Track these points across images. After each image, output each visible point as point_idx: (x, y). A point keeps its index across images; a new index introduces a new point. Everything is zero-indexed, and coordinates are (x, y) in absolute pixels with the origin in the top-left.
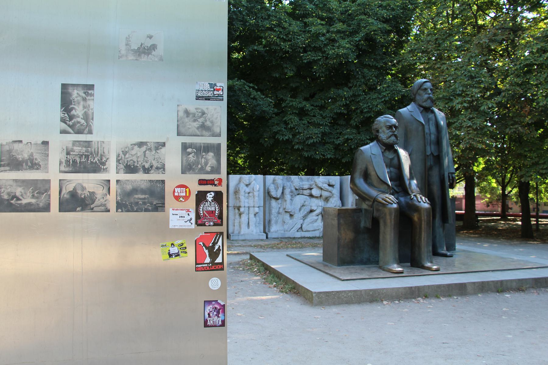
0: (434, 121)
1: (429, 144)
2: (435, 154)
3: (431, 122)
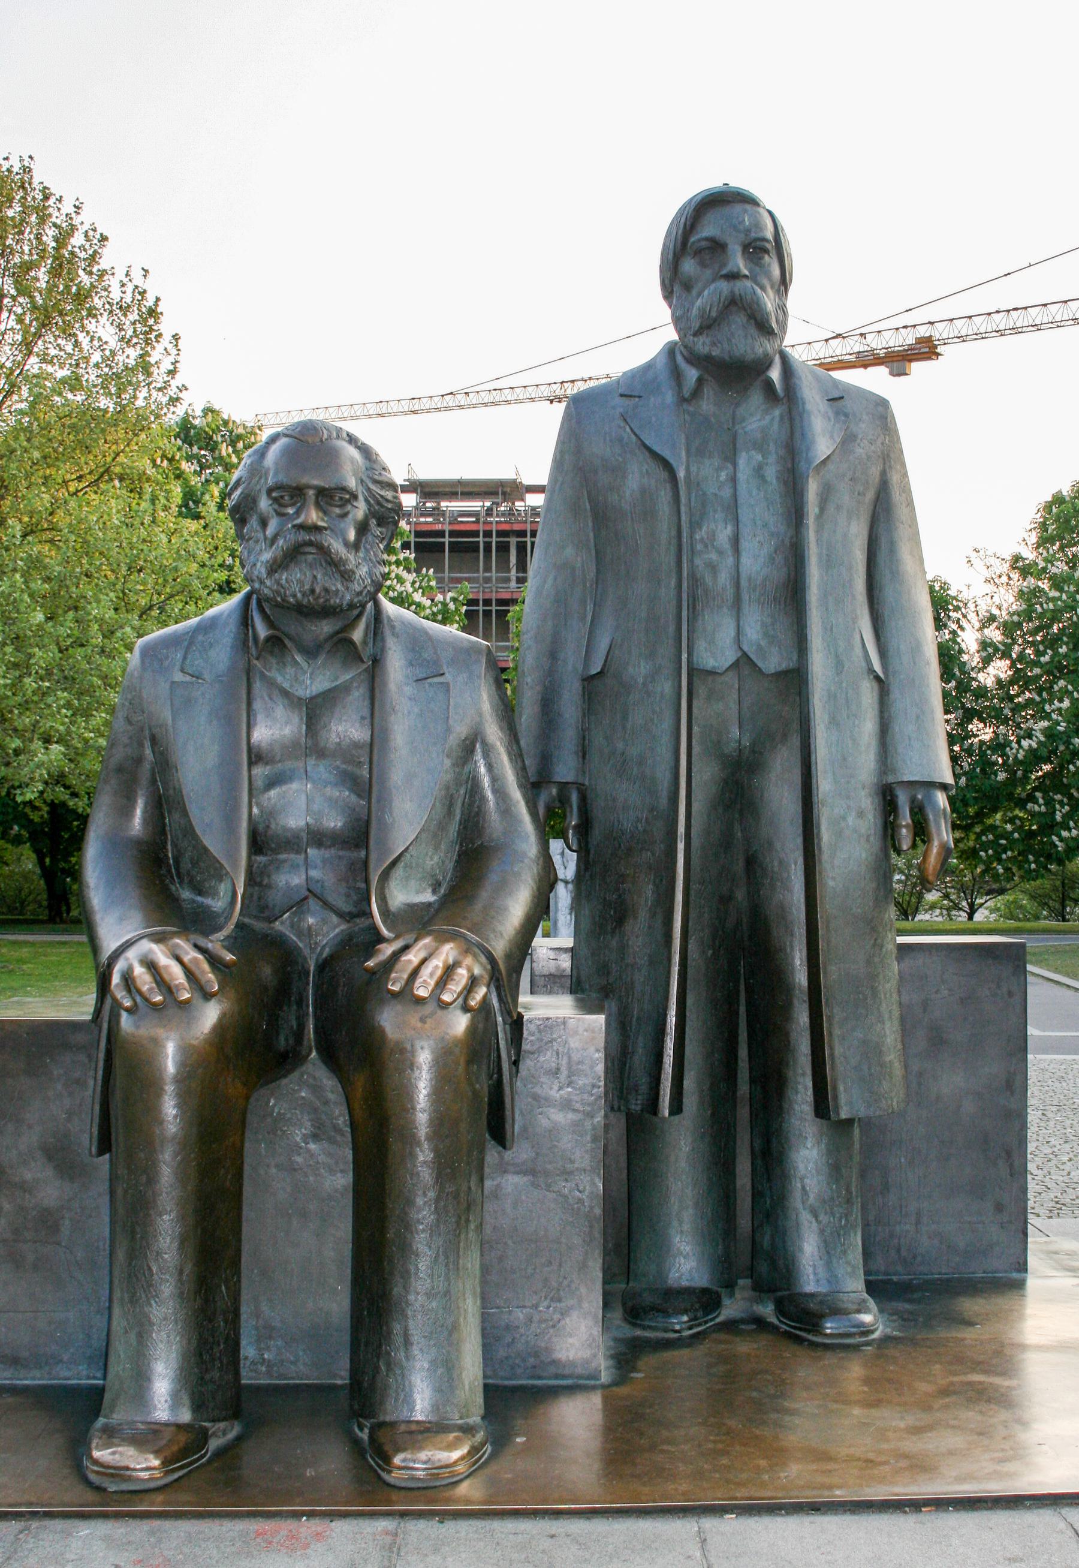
2: (773, 662)
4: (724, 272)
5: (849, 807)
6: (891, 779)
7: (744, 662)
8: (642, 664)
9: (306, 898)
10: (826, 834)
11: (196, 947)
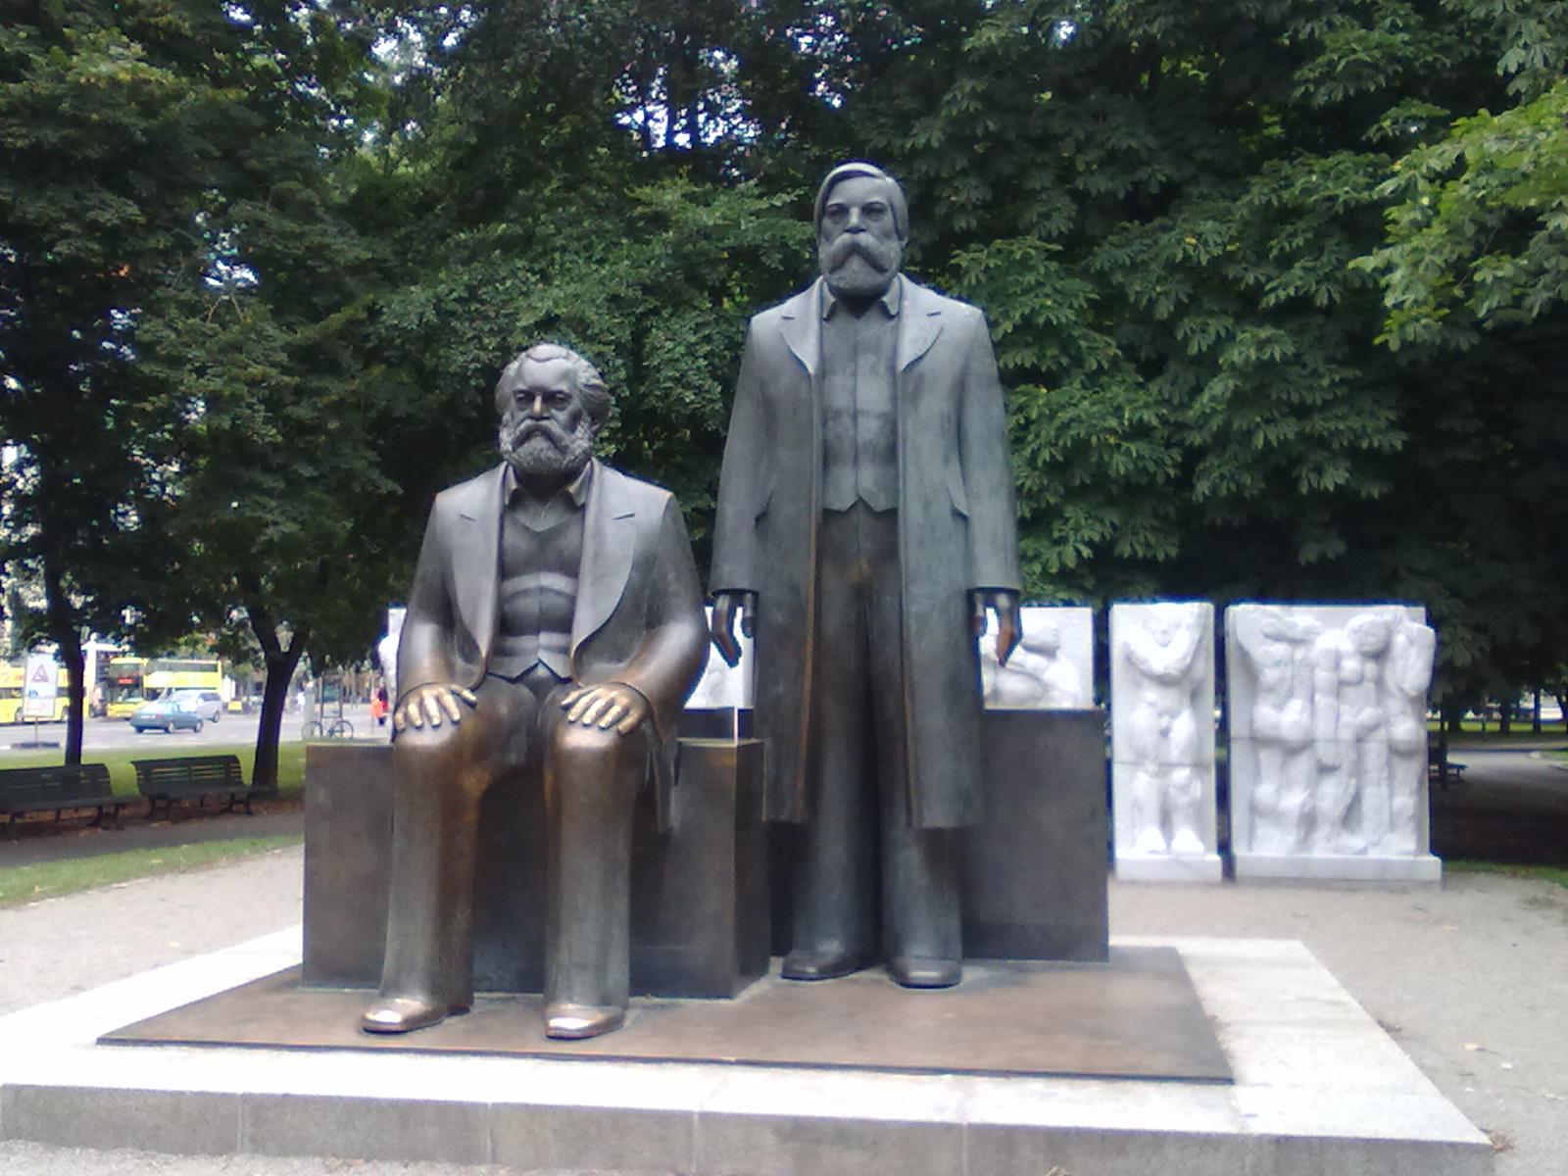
3: (866, 361)
4: (847, 228)
6: (972, 587)
7: (860, 502)
9: (536, 665)
11: (453, 693)
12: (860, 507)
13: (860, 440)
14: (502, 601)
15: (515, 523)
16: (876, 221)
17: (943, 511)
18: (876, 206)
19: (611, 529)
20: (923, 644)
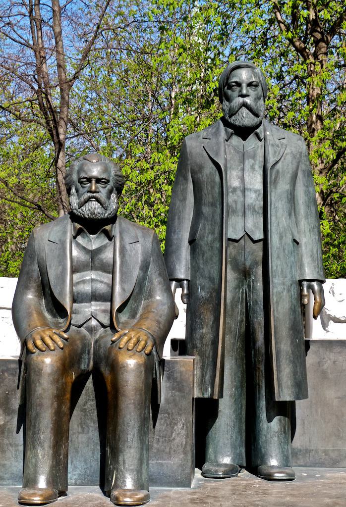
0: (260, 158)
1: (241, 214)
3: (248, 163)
5: (284, 289)
8: (210, 236)
9: (91, 318)
10: (274, 299)
12: (246, 235)
13: (246, 205)
14: (72, 284)
15: (78, 245)
16: (254, 91)
17: (289, 240)
18: (254, 83)
19: (128, 247)
20: (279, 308)
